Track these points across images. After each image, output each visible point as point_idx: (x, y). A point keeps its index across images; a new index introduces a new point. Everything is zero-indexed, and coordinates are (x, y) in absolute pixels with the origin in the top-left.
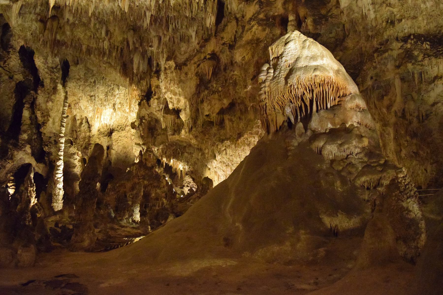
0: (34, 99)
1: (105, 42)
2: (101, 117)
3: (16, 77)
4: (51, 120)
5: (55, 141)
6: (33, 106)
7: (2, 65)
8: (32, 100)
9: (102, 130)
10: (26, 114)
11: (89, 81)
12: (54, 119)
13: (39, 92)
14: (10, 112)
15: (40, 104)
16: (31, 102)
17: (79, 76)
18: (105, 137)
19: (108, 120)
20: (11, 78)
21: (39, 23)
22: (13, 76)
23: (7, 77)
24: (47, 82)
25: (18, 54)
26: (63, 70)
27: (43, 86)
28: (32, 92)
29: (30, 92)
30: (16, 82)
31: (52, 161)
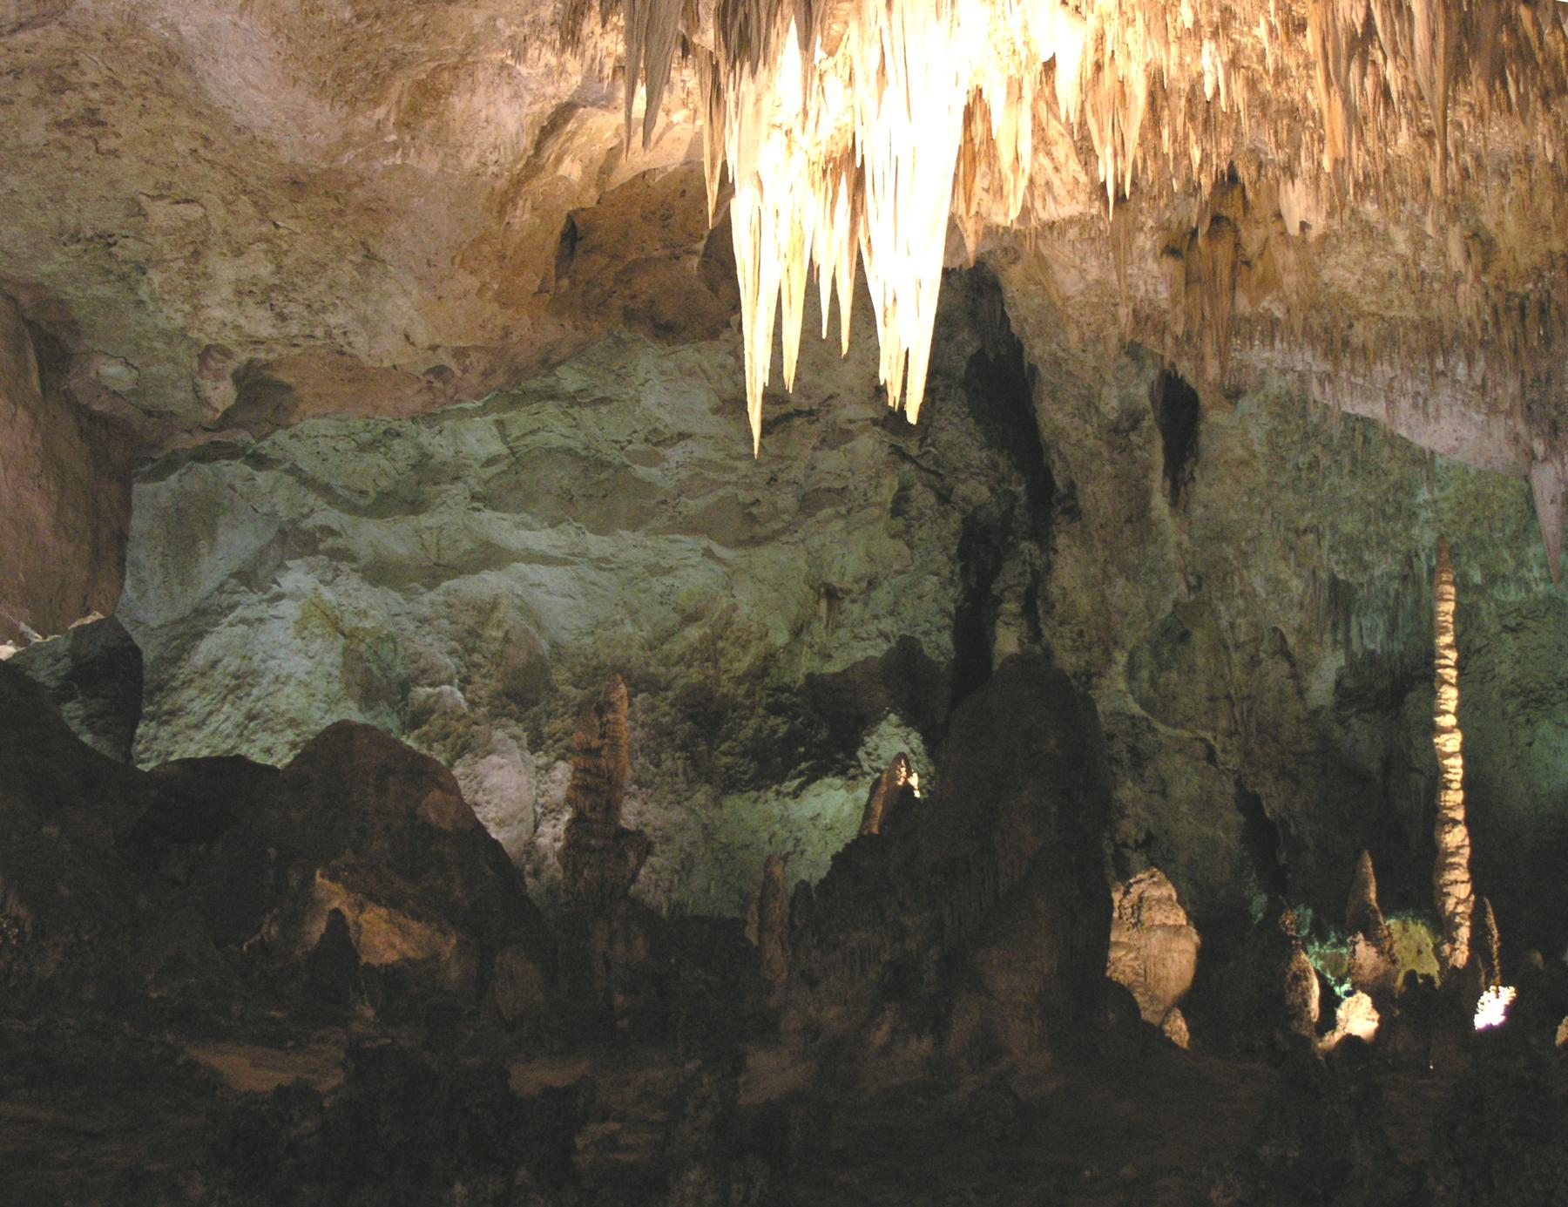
0: (1035, 574)
1: (1462, 288)
2: (1348, 623)
3: (962, 489)
4: (1121, 658)
5: (1133, 750)
6: (1034, 601)
7: (914, 452)
8: (1028, 578)
9: (1349, 683)
10: (1007, 641)
11: (1289, 466)
12: (1131, 655)
13: (1061, 541)
14: (946, 639)
15: (1065, 596)
16: (1022, 590)
17: (1247, 449)
18: (1367, 716)
19: (1380, 636)
20: (944, 497)
21: (1169, 264)
22: (951, 491)
23: (932, 499)
24: (1097, 495)
25: (962, 394)
26: (1165, 434)
27: (1074, 513)
28: (1025, 546)
29: (1014, 545)
30: (963, 511)
31: (1125, 845)
